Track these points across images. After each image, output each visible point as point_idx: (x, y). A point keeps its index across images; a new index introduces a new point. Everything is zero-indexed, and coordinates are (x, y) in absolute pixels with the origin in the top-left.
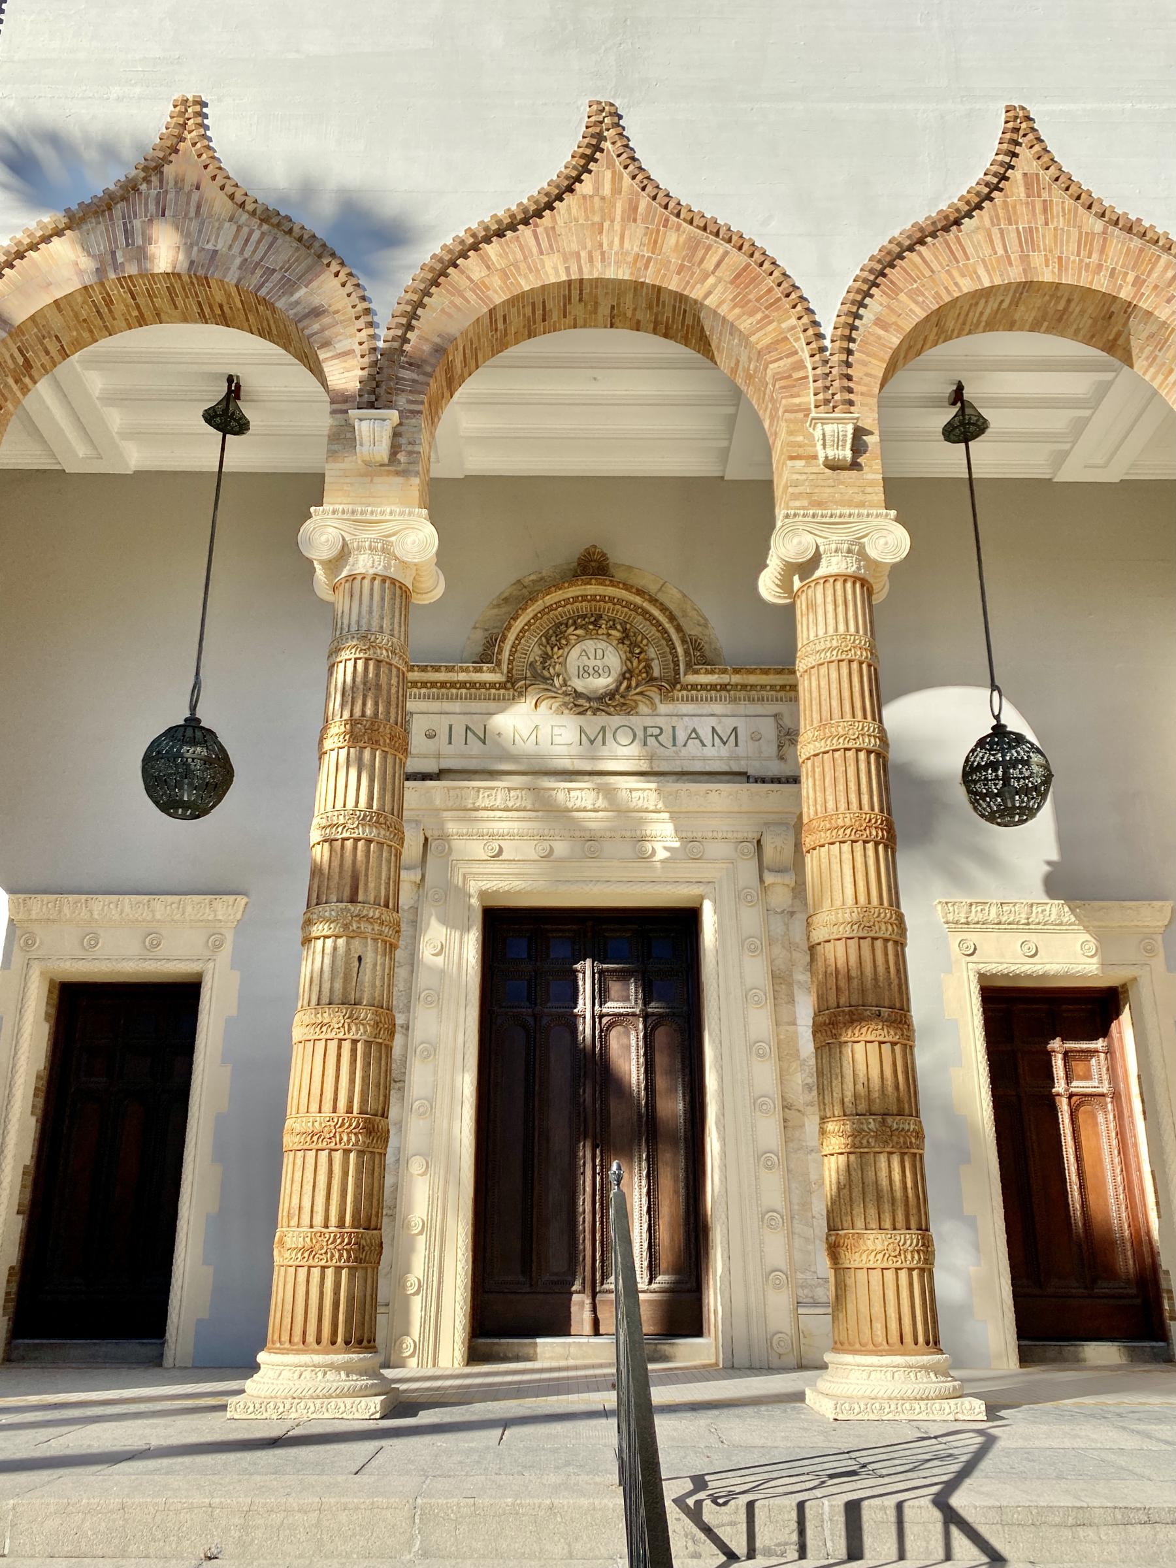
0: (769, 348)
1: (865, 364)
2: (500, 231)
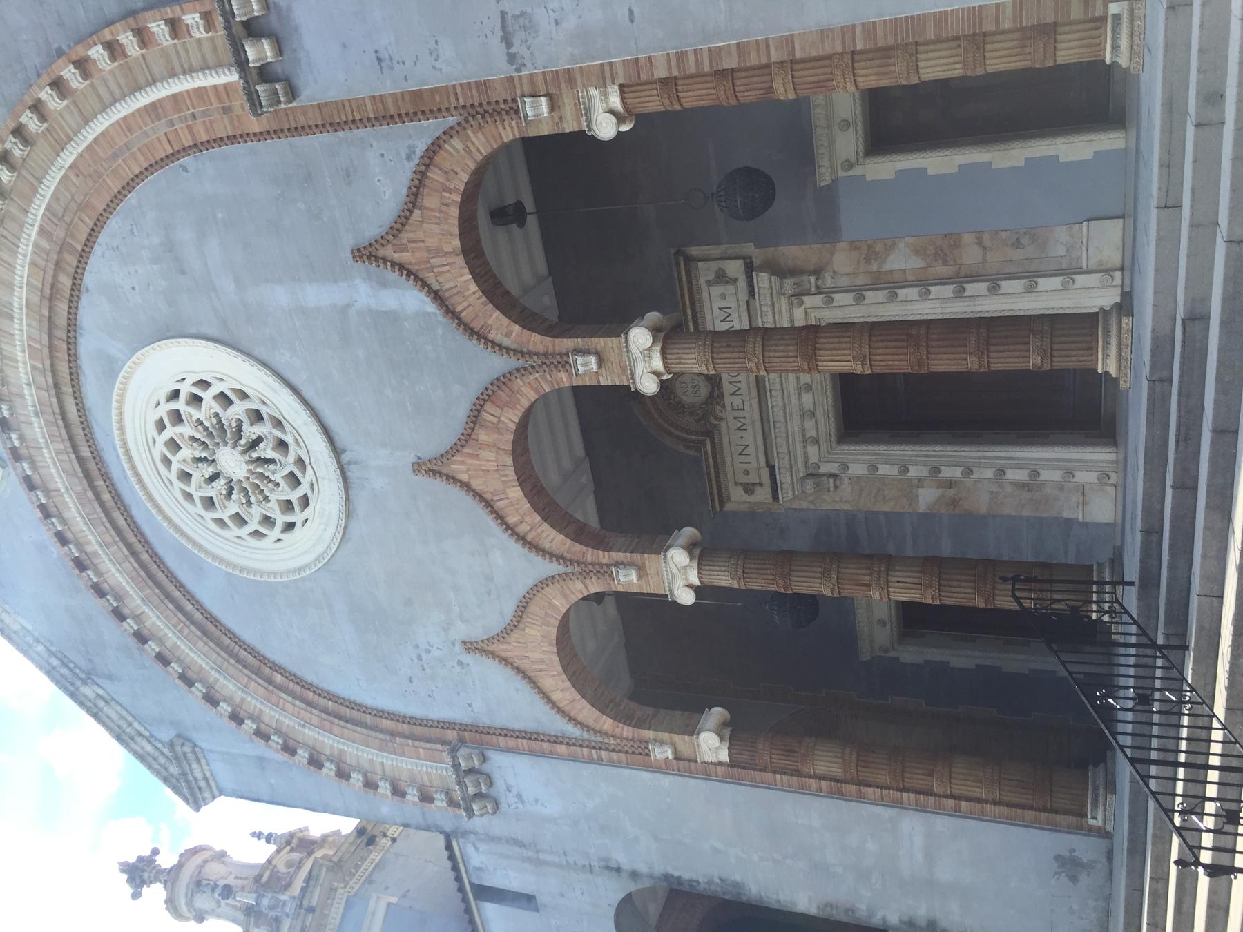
1: (535, 343)
2: (500, 517)
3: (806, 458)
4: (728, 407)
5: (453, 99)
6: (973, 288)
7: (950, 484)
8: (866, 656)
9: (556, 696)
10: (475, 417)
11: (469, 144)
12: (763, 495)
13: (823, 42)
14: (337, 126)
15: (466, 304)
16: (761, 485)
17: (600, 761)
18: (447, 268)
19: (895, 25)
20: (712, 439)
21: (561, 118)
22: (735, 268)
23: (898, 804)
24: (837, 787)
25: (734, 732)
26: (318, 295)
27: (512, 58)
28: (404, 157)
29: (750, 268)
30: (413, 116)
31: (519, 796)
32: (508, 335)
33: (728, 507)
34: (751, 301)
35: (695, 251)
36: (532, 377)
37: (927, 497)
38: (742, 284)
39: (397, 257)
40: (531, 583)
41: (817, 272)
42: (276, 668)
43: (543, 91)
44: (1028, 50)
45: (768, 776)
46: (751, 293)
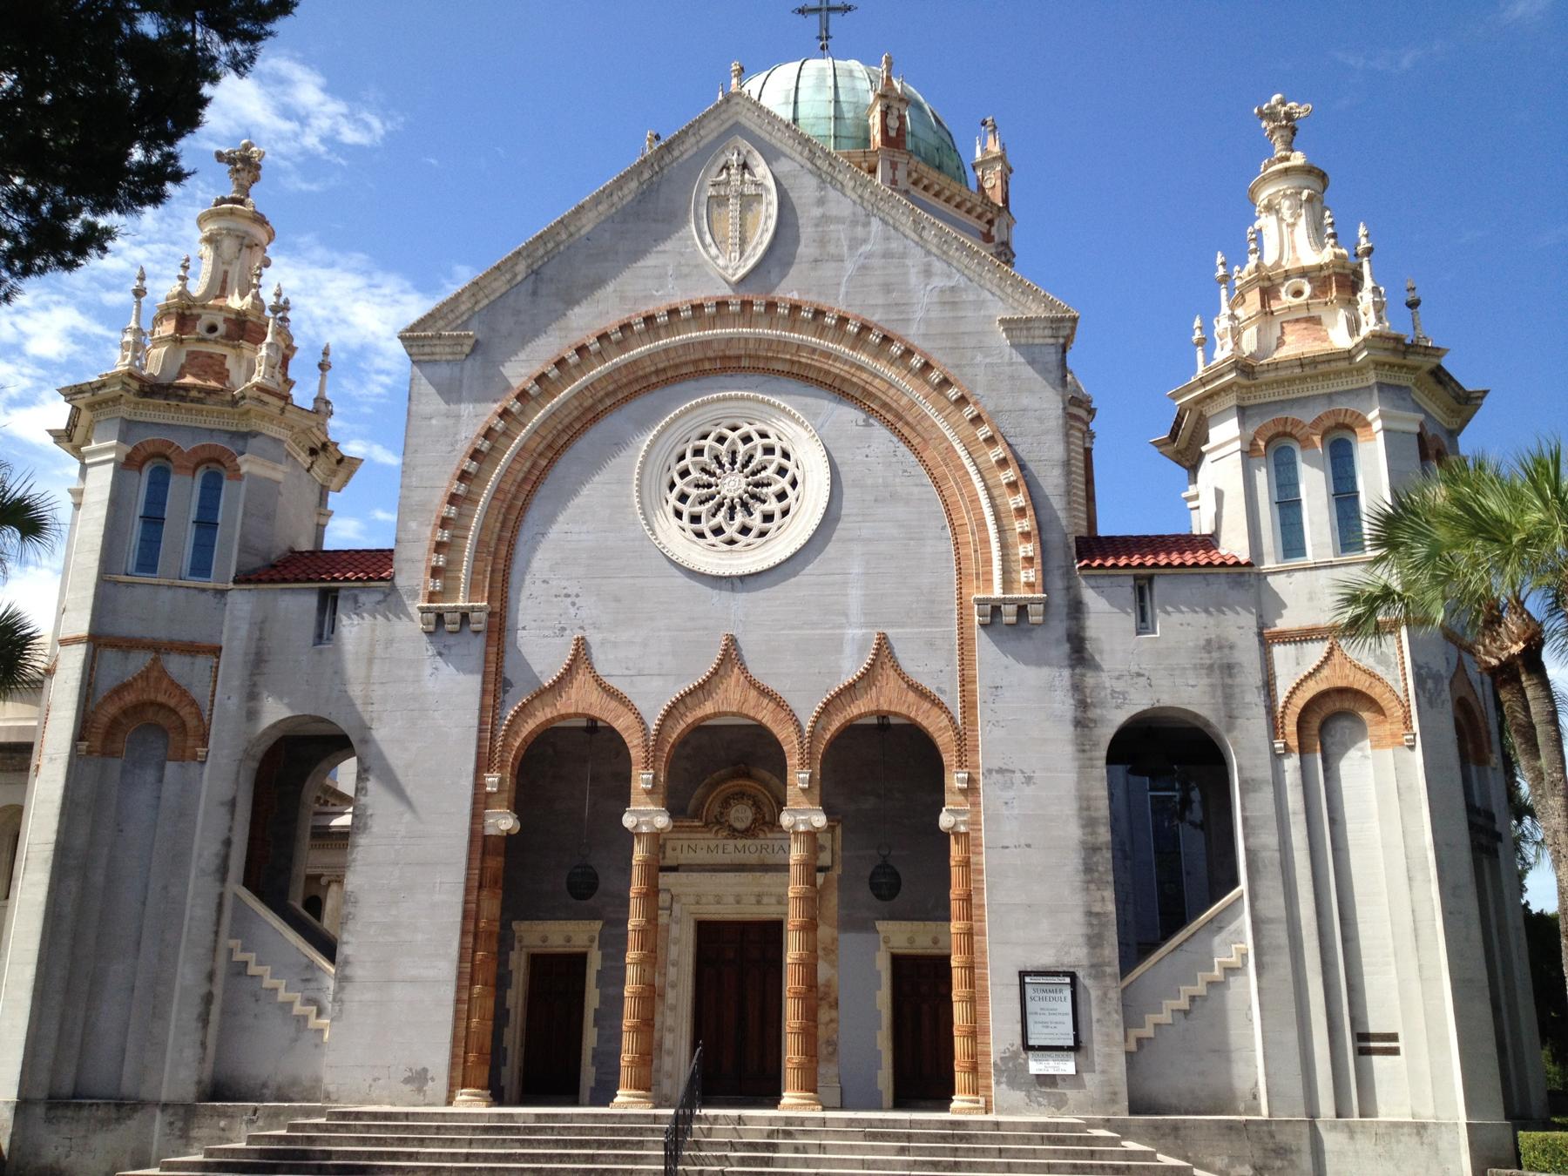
10: (764, 692)
17: (481, 731)
26: (855, 598)
42: (552, 462)
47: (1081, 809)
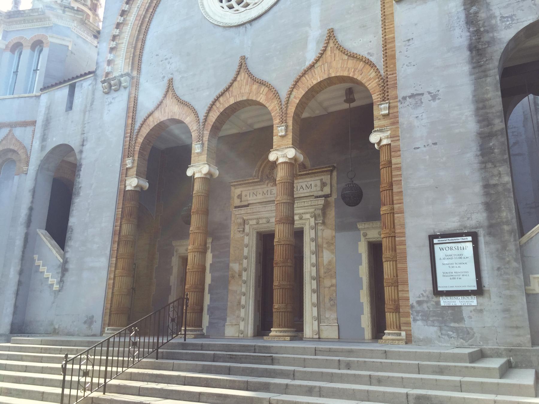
0: (272, 110)
1: (291, 109)
2: (222, 94)
3: (251, 219)
4: (272, 188)
5: (391, 73)
6: (314, 283)
7: (240, 275)
8: (174, 243)
9: (151, 118)
10: (262, 83)
11: (372, 80)
12: (237, 202)
13: (400, 225)
14: (384, 21)
15: (308, 79)
16: (241, 201)
17: (125, 137)
18: (323, 71)
19: (404, 253)
20: (260, 182)
21: (380, 119)
22: (327, 190)
23: (111, 256)
24: (117, 233)
25: (139, 192)
27: (404, 98)
28: (369, 51)
29: (326, 196)
30: (385, 55)
31: (111, 103)
32: (295, 97)
33: (233, 188)
34: (313, 197)
35: (335, 174)
36: (277, 107)
37: (235, 267)
38: (321, 193)
39: (329, 48)
40: (196, 107)
41: (324, 223)
43: (391, 111)
44: (391, 302)
45: (121, 206)
46: (317, 197)
47: (477, 109)
